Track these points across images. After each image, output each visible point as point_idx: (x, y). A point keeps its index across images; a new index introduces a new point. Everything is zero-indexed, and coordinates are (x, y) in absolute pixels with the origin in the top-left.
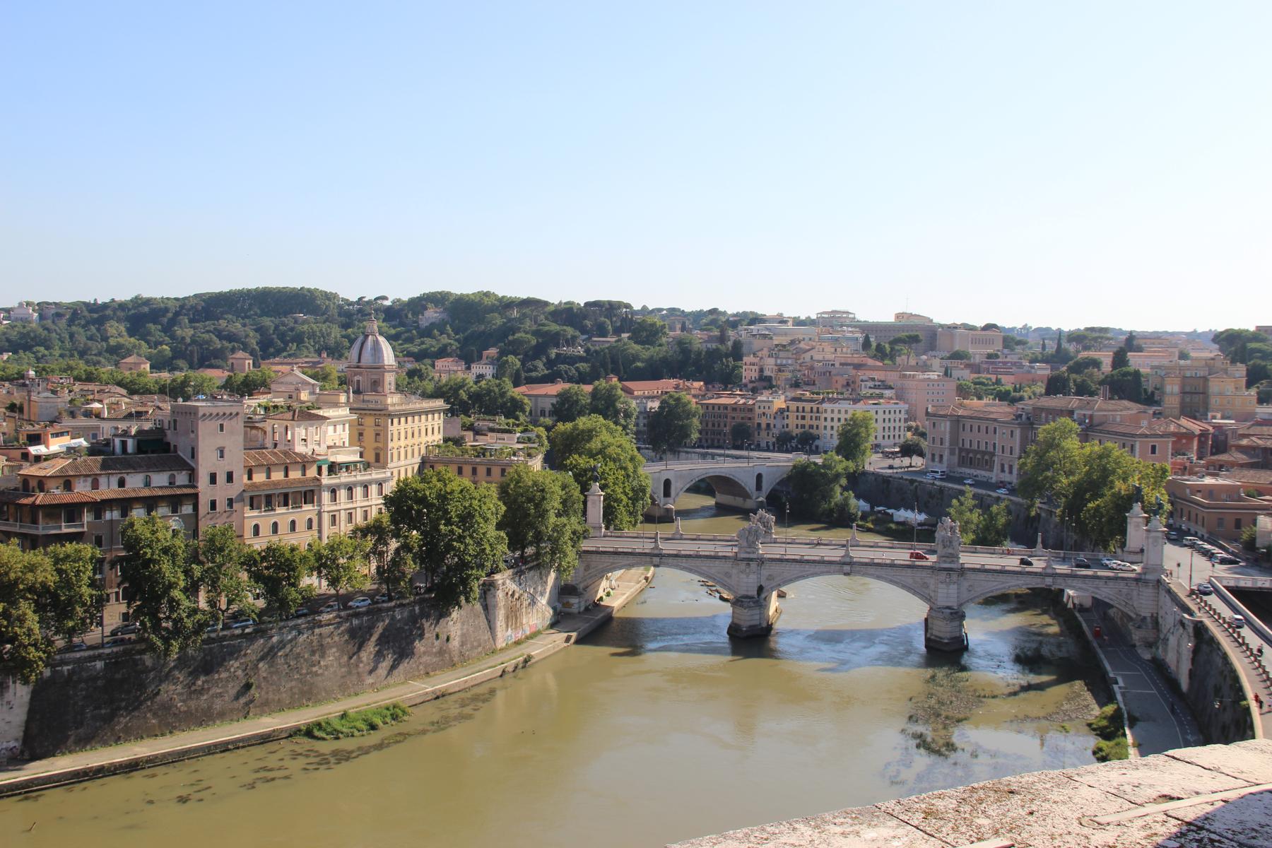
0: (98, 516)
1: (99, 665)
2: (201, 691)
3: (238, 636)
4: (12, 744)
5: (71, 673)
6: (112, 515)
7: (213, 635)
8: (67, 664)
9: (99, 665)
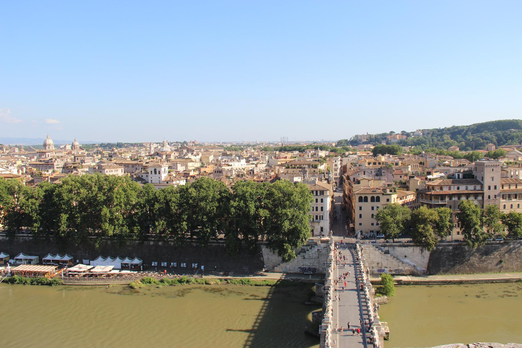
0: (450, 199)
1: (451, 248)
2: (484, 261)
3: (498, 244)
4: (424, 269)
5: (442, 249)
6: (455, 199)
7: (489, 242)
8: (441, 246)
9: (451, 248)
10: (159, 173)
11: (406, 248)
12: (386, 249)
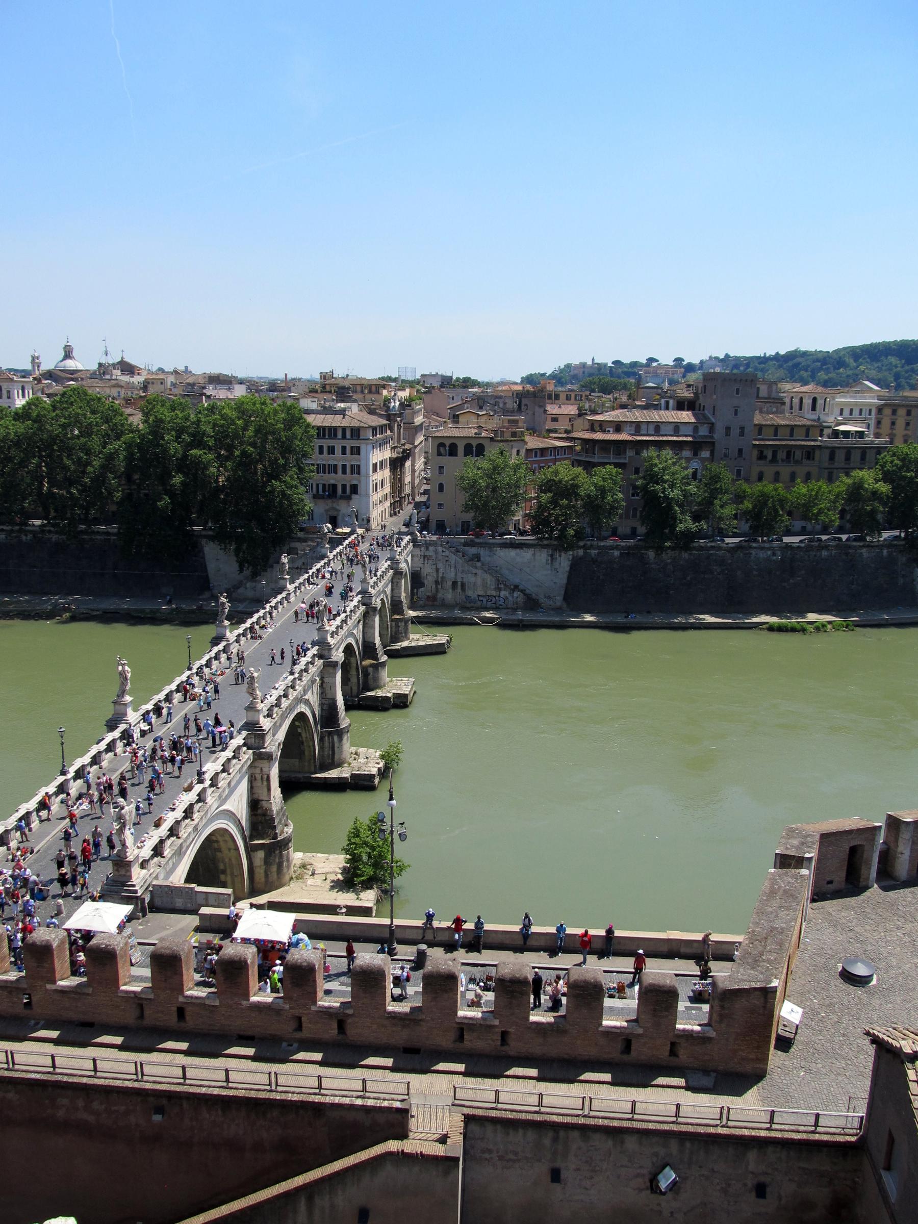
0: (638, 453)
1: (616, 553)
8: (594, 549)
9: (616, 553)
10: (9, 398)
11: (518, 551)
12: (473, 550)
